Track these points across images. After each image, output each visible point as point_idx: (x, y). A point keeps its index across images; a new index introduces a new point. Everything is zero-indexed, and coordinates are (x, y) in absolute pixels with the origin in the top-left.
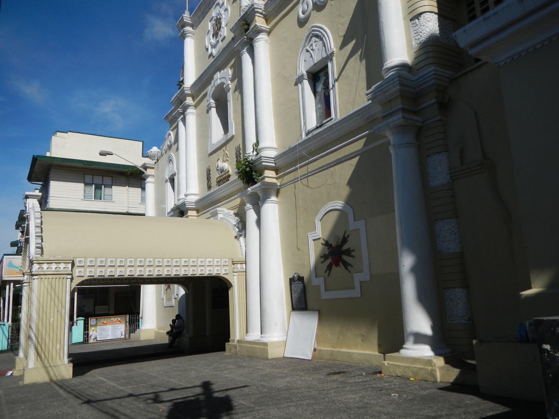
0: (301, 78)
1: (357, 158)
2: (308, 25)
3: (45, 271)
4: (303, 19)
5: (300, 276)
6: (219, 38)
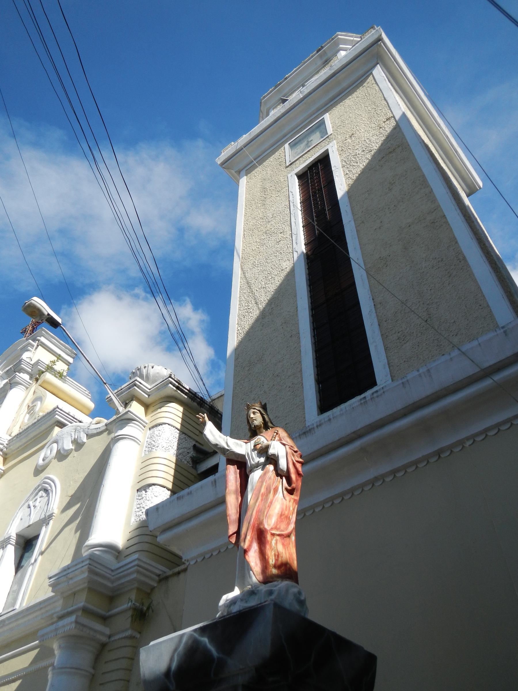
0: (6, 541)
1: (18, 683)
2: (43, 475)
4: (42, 466)
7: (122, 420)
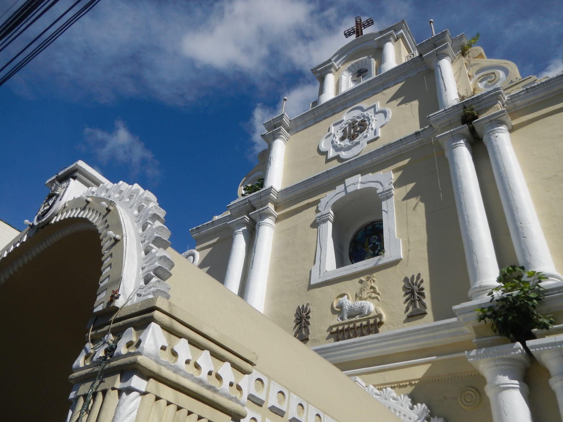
3: (177, 370)
6: (362, 140)
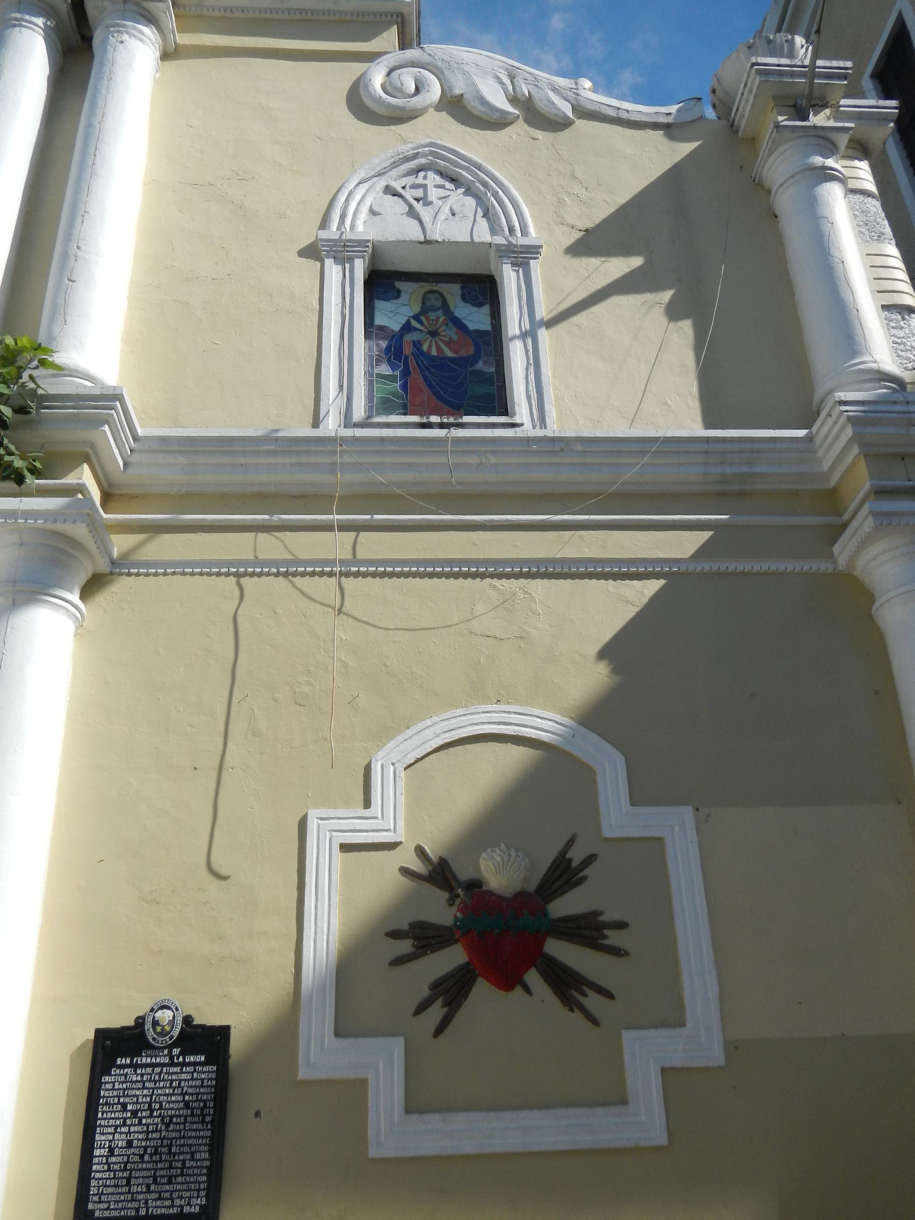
5: (198, 1021)
7: (824, 138)
